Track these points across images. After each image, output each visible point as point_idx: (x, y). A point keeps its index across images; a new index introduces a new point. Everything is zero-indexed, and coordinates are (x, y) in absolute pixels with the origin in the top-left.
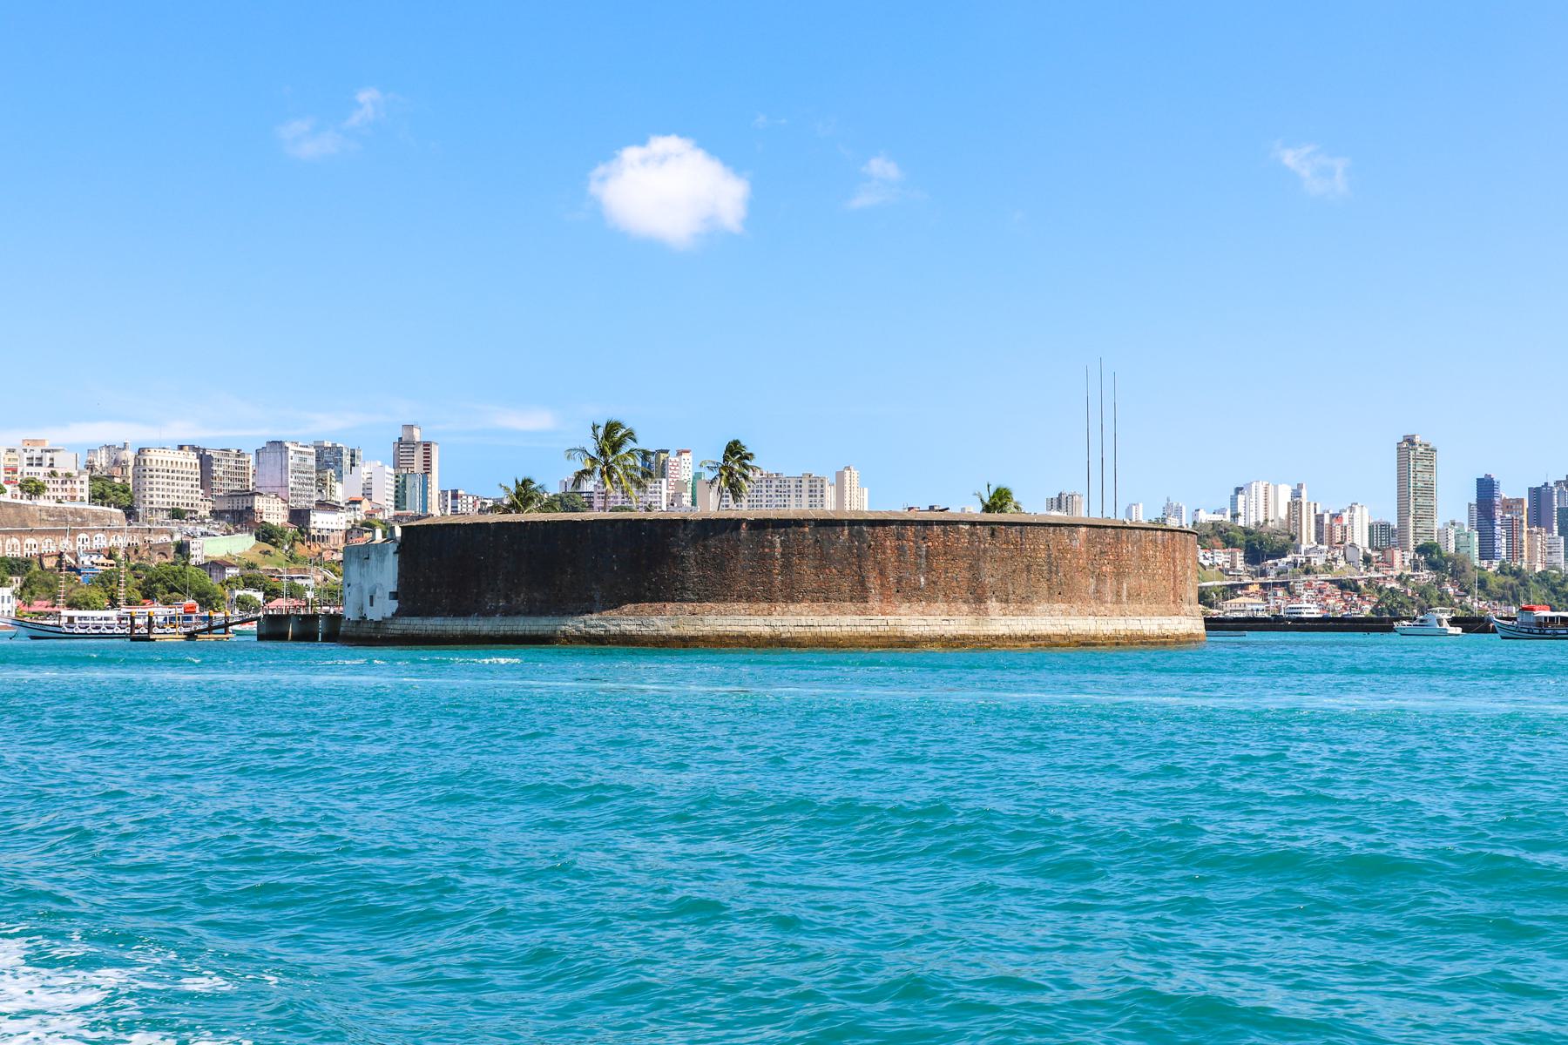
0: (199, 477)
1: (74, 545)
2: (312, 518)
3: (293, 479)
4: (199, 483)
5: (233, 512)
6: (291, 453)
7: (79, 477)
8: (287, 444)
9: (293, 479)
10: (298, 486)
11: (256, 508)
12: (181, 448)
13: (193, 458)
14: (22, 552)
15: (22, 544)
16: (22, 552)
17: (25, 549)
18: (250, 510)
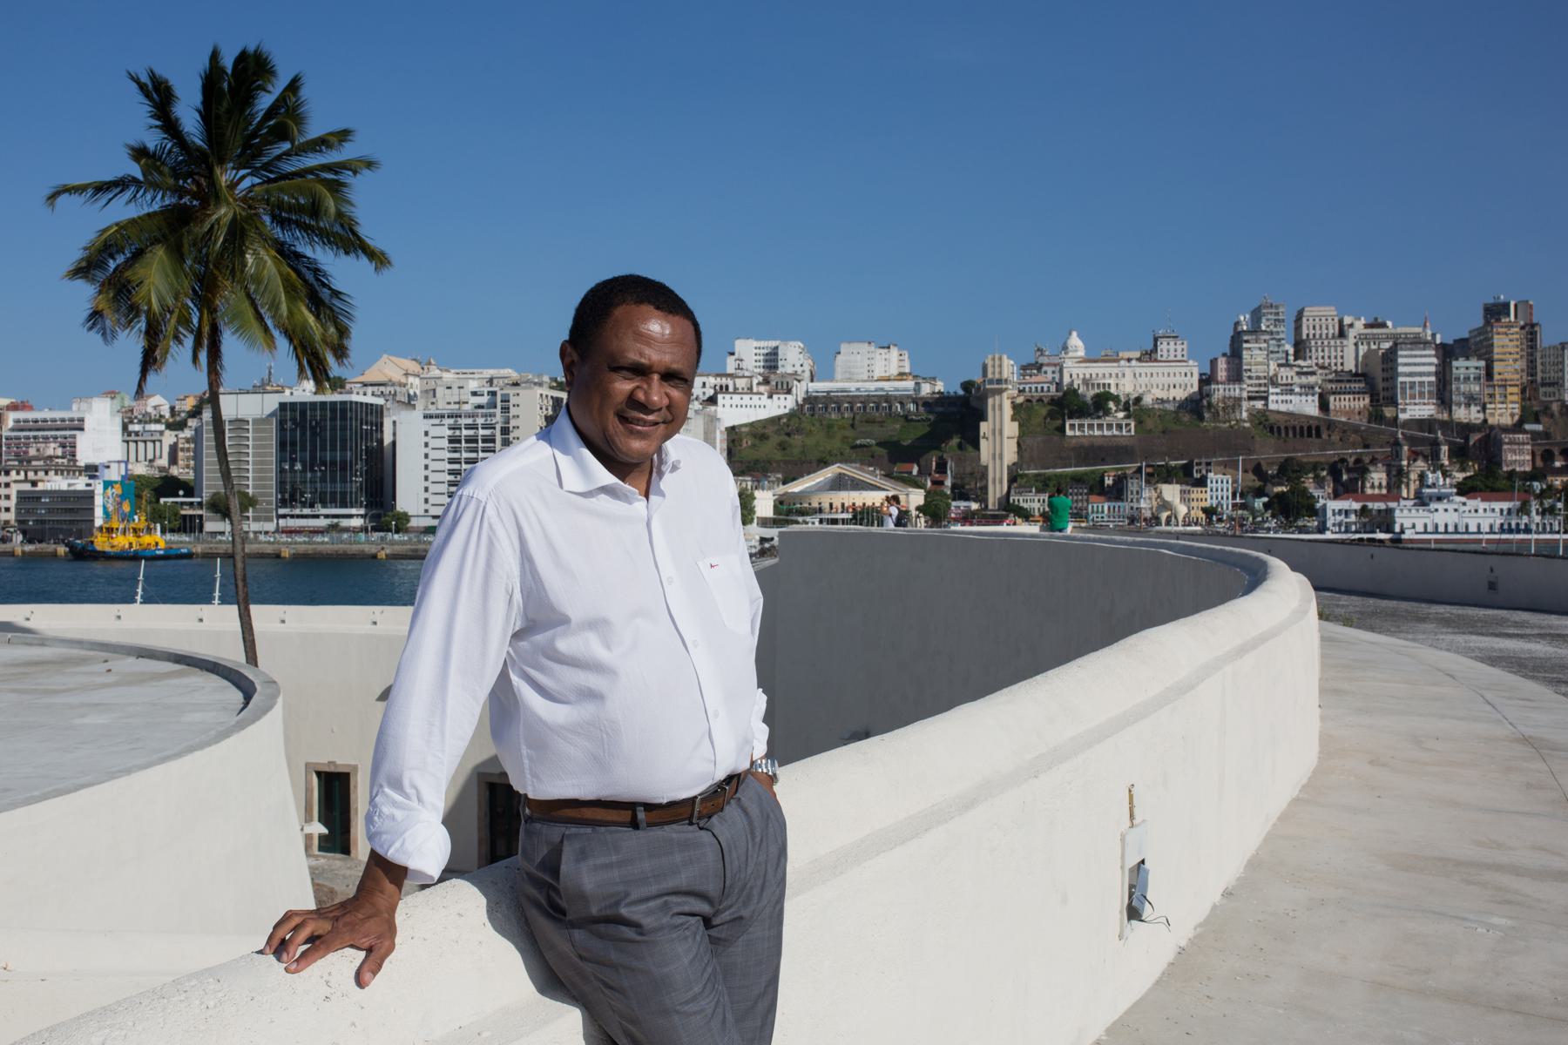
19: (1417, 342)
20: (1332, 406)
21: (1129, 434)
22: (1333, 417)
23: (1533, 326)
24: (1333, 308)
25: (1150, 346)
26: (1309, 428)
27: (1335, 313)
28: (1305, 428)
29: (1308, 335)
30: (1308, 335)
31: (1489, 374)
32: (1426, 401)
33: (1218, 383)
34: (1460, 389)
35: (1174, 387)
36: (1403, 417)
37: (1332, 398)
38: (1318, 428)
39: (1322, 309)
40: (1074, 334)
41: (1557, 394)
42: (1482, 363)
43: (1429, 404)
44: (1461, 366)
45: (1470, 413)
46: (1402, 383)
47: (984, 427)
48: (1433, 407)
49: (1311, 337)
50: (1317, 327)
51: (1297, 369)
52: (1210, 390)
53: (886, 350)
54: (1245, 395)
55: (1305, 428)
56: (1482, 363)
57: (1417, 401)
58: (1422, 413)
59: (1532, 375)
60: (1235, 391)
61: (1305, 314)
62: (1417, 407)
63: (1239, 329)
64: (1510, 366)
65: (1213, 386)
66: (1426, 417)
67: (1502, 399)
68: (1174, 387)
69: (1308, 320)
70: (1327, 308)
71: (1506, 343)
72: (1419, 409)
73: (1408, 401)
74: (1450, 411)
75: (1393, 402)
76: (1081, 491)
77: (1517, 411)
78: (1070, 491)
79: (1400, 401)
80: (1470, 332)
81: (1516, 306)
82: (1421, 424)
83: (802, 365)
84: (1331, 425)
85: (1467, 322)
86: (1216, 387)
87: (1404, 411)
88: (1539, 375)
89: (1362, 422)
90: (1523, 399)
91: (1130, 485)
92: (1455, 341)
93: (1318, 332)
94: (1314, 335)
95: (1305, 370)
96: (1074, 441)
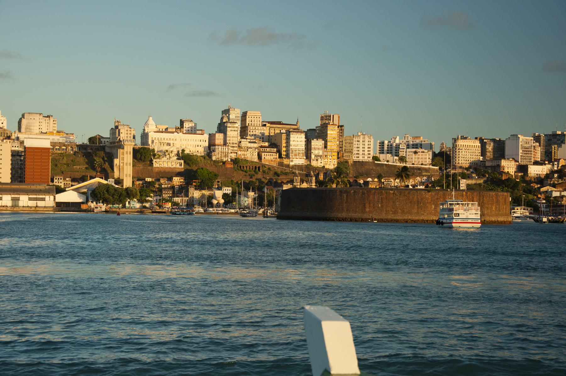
0: (480, 151)
1: (415, 181)
2: (529, 169)
3: (522, 152)
4: (480, 154)
5: (491, 167)
6: (521, 140)
7: (428, 152)
8: (519, 136)
9: (522, 152)
10: (524, 155)
11: (502, 165)
12: (476, 138)
13: (478, 143)
14: (394, 184)
15: (394, 182)
16: (394, 184)
17: (395, 183)
18: (499, 166)
19: (297, 131)
20: (263, 158)
21: (181, 167)
22: (263, 162)
23: (342, 126)
24: (260, 112)
25: (179, 125)
26: (256, 167)
27: (260, 115)
28: (254, 167)
29: (249, 124)
30: (249, 124)
31: (326, 147)
32: (301, 157)
33: (218, 145)
34: (314, 152)
35: (198, 146)
36: (292, 164)
37: (263, 154)
38: (259, 168)
39: (255, 112)
40: (151, 118)
41: (350, 156)
42: (323, 142)
43: (302, 158)
44: (317, 144)
45: (318, 163)
46: (291, 149)
47: (116, 161)
48: (303, 160)
49: (250, 125)
50: (253, 121)
51: (249, 140)
52: (215, 148)
53: (48, 119)
54: (230, 151)
55: (254, 167)
56: (323, 142)
57: (297, 157)
58: (299, 162)
59: (341, 148)
60: (225, 149)
61: (248, 114)
62: (297, 160)
63: (224, 121)
64: (333, 145)
65: (216, 147)
66: (301, 164)
67: (331, 157)
68: (198, 146)
69: (249, 117)
70: (257, 112)
71: (332, 132)
72: (299, 161)
73: (294, 157)
74: (310, 162)
75: (288, 156)
76: (166, 192)
77: (336, 163)
78: (164, 192)
79: (290, 157)
80: (316, 127)
81: (333, 116)
82: (299, 167)
83: (2, 123)
84: (264, 166)
85: (315, 123)
86: (218, 147)
87: (292, 161)
88: (344, 148)
89: (275, 164)
90: (338, 158)
91: (190, 190)
92: (308, 130)
93: (253, 123)
94: (251, 124)
95: (252, 140)
96: (157, 169)
